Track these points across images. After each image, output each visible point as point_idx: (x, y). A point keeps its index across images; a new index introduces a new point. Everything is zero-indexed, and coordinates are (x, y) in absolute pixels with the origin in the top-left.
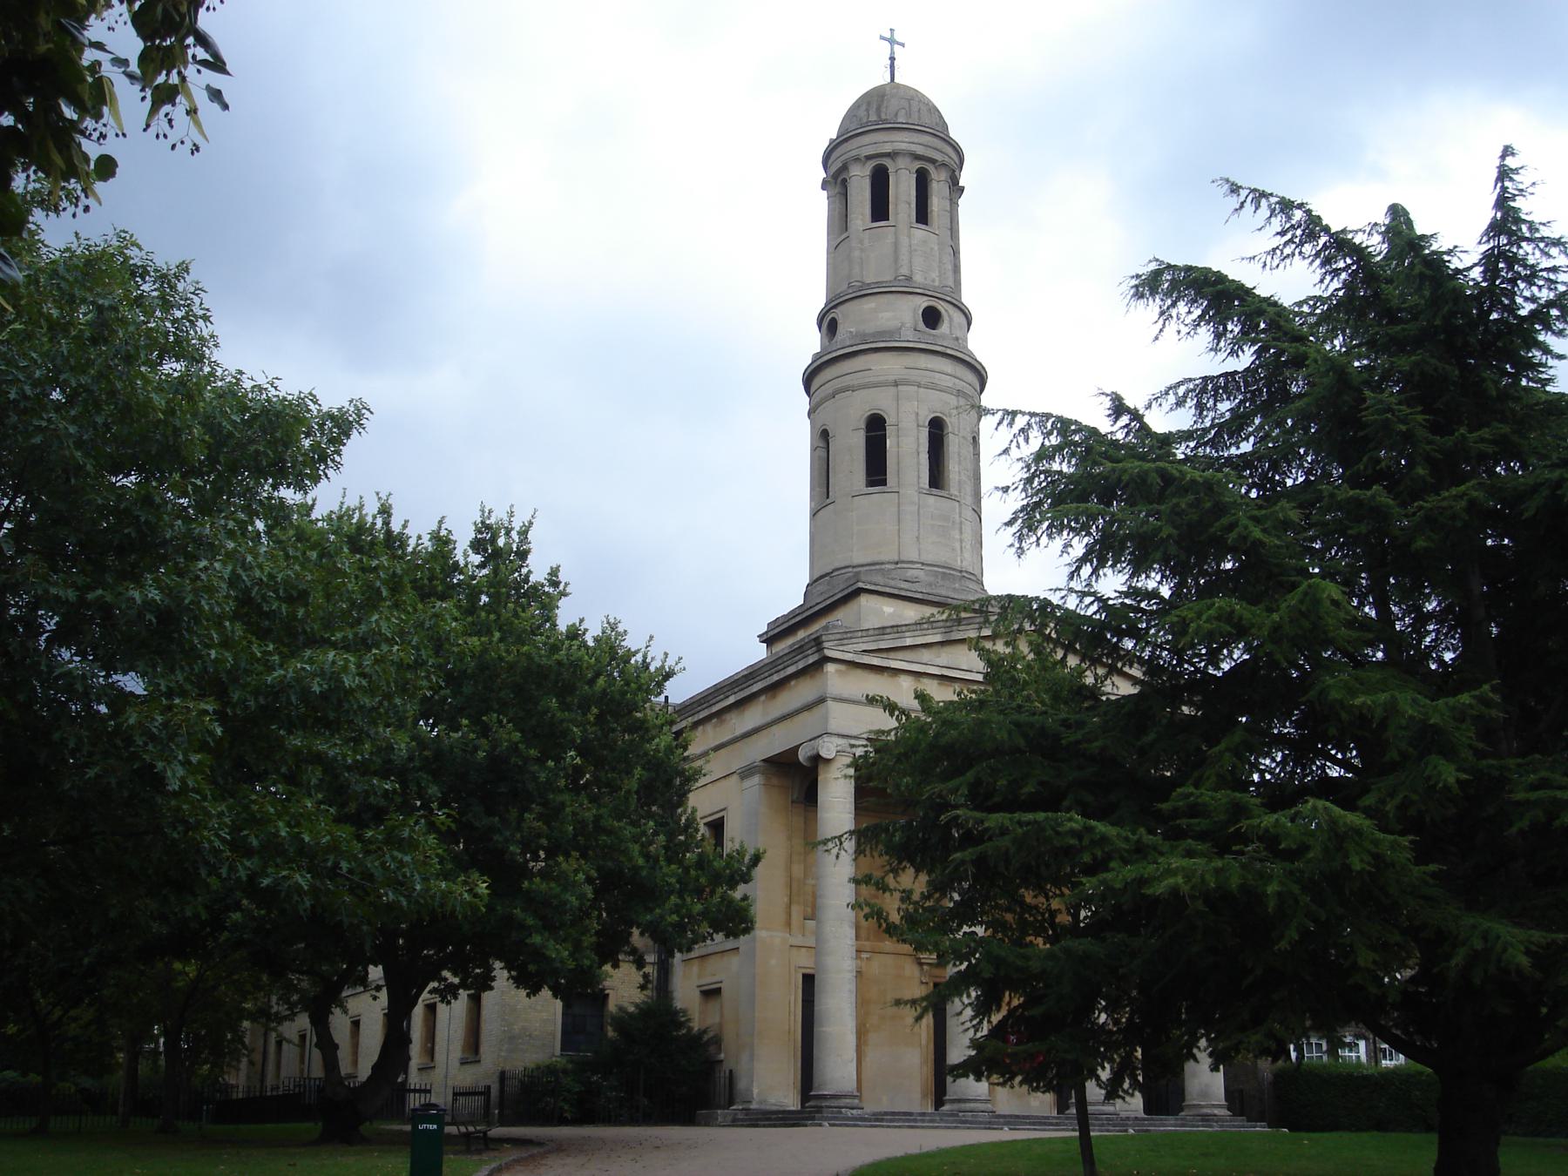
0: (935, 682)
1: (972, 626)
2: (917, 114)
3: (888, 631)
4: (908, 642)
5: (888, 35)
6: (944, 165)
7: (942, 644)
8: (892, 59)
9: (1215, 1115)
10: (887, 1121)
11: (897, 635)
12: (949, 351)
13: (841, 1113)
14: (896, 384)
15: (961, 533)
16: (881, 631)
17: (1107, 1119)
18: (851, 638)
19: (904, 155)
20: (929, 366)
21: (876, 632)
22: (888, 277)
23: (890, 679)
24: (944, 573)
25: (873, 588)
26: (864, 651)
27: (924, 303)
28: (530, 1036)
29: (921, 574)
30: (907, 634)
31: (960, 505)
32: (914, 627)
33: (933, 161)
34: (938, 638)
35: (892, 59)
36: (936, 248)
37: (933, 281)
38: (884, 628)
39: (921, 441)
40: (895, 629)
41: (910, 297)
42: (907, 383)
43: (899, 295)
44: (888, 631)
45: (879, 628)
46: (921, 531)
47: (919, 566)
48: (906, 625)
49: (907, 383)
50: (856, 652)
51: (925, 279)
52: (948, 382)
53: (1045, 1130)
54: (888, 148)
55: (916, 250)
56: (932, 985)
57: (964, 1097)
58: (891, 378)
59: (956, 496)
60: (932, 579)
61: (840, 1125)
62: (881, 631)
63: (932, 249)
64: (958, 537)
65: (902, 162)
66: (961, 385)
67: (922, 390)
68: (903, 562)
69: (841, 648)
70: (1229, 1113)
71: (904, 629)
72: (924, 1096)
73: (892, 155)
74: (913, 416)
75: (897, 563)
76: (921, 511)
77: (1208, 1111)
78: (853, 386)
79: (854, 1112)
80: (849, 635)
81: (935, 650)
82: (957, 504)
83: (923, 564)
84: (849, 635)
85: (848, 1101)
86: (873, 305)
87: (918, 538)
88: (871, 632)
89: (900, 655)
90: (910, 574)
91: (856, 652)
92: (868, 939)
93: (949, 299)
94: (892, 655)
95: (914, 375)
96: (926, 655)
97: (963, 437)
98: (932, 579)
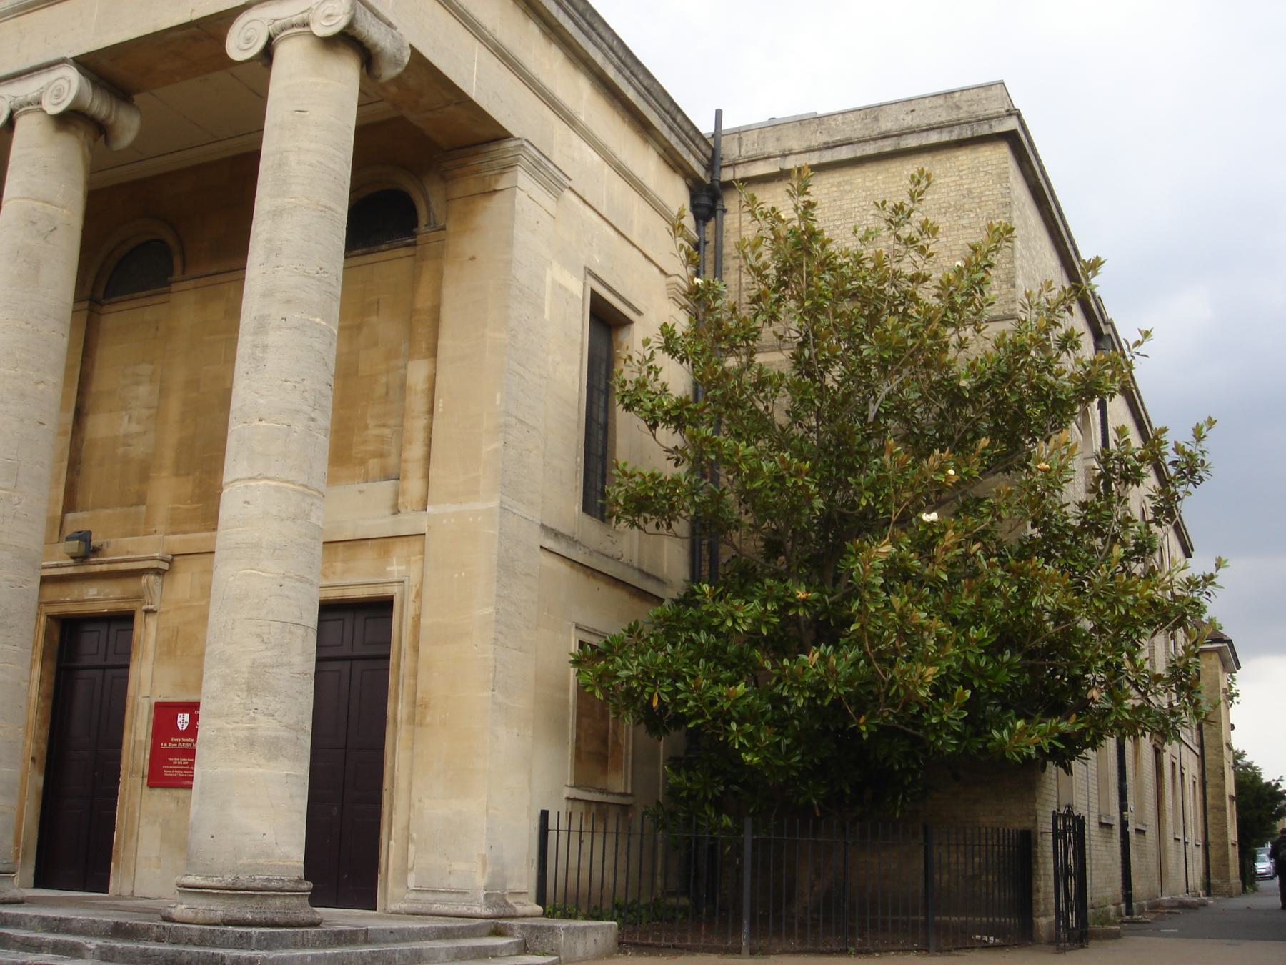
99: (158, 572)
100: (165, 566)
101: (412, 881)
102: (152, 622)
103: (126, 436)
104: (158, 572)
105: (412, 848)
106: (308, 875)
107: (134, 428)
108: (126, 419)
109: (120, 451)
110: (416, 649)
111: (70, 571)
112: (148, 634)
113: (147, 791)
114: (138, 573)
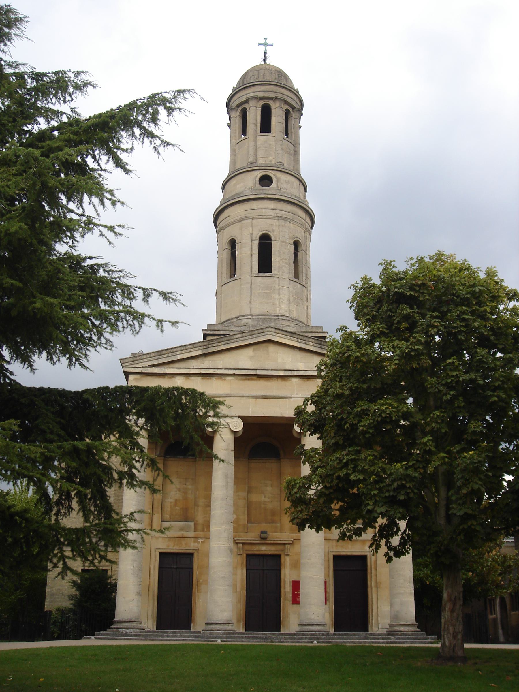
0: (199, 378)
1: (222, 343)
2: (262, 76)
3: (164, 352)
4: (179, 357)
5: (263, 42)
6: (276, 98)
7: (206, 355)
8: (265, 53)
9: (400, 631)
10: (143, 636)
11: (170, 354)
12: (270, 196)
13: (118, 631)
14: (241, 220)
15: (279, 294)
16: (159, 353)
17: (312, 635)
18: (140, 359)
19: (251, 99)
20: (259, 207)
21: (156, 354)
22: (245, 164)
23: (170, 379)
24: (264, 319)
25: (212, 333)
26: (149, 366)
27: (260, 174)
28: (62, 593)
29: (249, 321)
30: (178, 353)
31: (279, 281)
32: (182, 348)
33: (271, 98)
34: (199, 353)
35: (265, 53)
36: (273, 144)
37: (271, 161)
38: (160, 351)
39: (254, 248)
40: (169, 351)
41: (252, 172)
42: (246, 218)
43: (247, 173)
44: (164, 352)
45: (157, 352)
46: (253, 297)
47: (250, 317)
48: (175, 348)
49: (246, 218)
50: (143, 367)
51: (266, 161)
52: (272, 213)
53: (127, 639)
54: (244, 99)
55: (260, 147)
56: (245, 555)
57: (210, 622)
58: (238, 218)
59: (277, 275)
60: (256, 323)
61: (104, 639)
62: (159, 353)
63: (270, 145)
64: (277, 297)
65: (251, 103)
66: (280, 213)
67: (255, 221)
68: (240, 316)
69: (134, 366)
70: (418, 630)
71: (174, 350)
72: (238, 621)
73: (247, 101)
74: (249, 236)
75: (238, 317)
76: (253, 287)
77: (397, 628)
78: (223, 227)
79: (127, 631)
80: (138, 358)
81: (200, 360)
82: (277, 279)
83: (252, 315)
84: (138, 358)
85: (126, 624)
86: (234, 182)
87: (250, 302)
88: (152, 355)
89: (177, 365)
90: (243, 322)
91: (143, 367)
92: (203, 531)
93: (276, 168)
94: (171, 366)
95: (251, 214)
96: (194, 363)
97: (283, 242)
98: (256, 323)
99: (290, 544)
100: (291, 542)
101: (380, 626)
102: (288, 559)
103: (264, 502)
104: (290, 544)
105: (379, 618)
106: (416, 621)
107: (267, 500)
108: (263, 496)
109: (263, 506)
110: (376, 569)
111: (258, 542)
112: (287, 561)
113: (292, 605)
114: (285, 544)
